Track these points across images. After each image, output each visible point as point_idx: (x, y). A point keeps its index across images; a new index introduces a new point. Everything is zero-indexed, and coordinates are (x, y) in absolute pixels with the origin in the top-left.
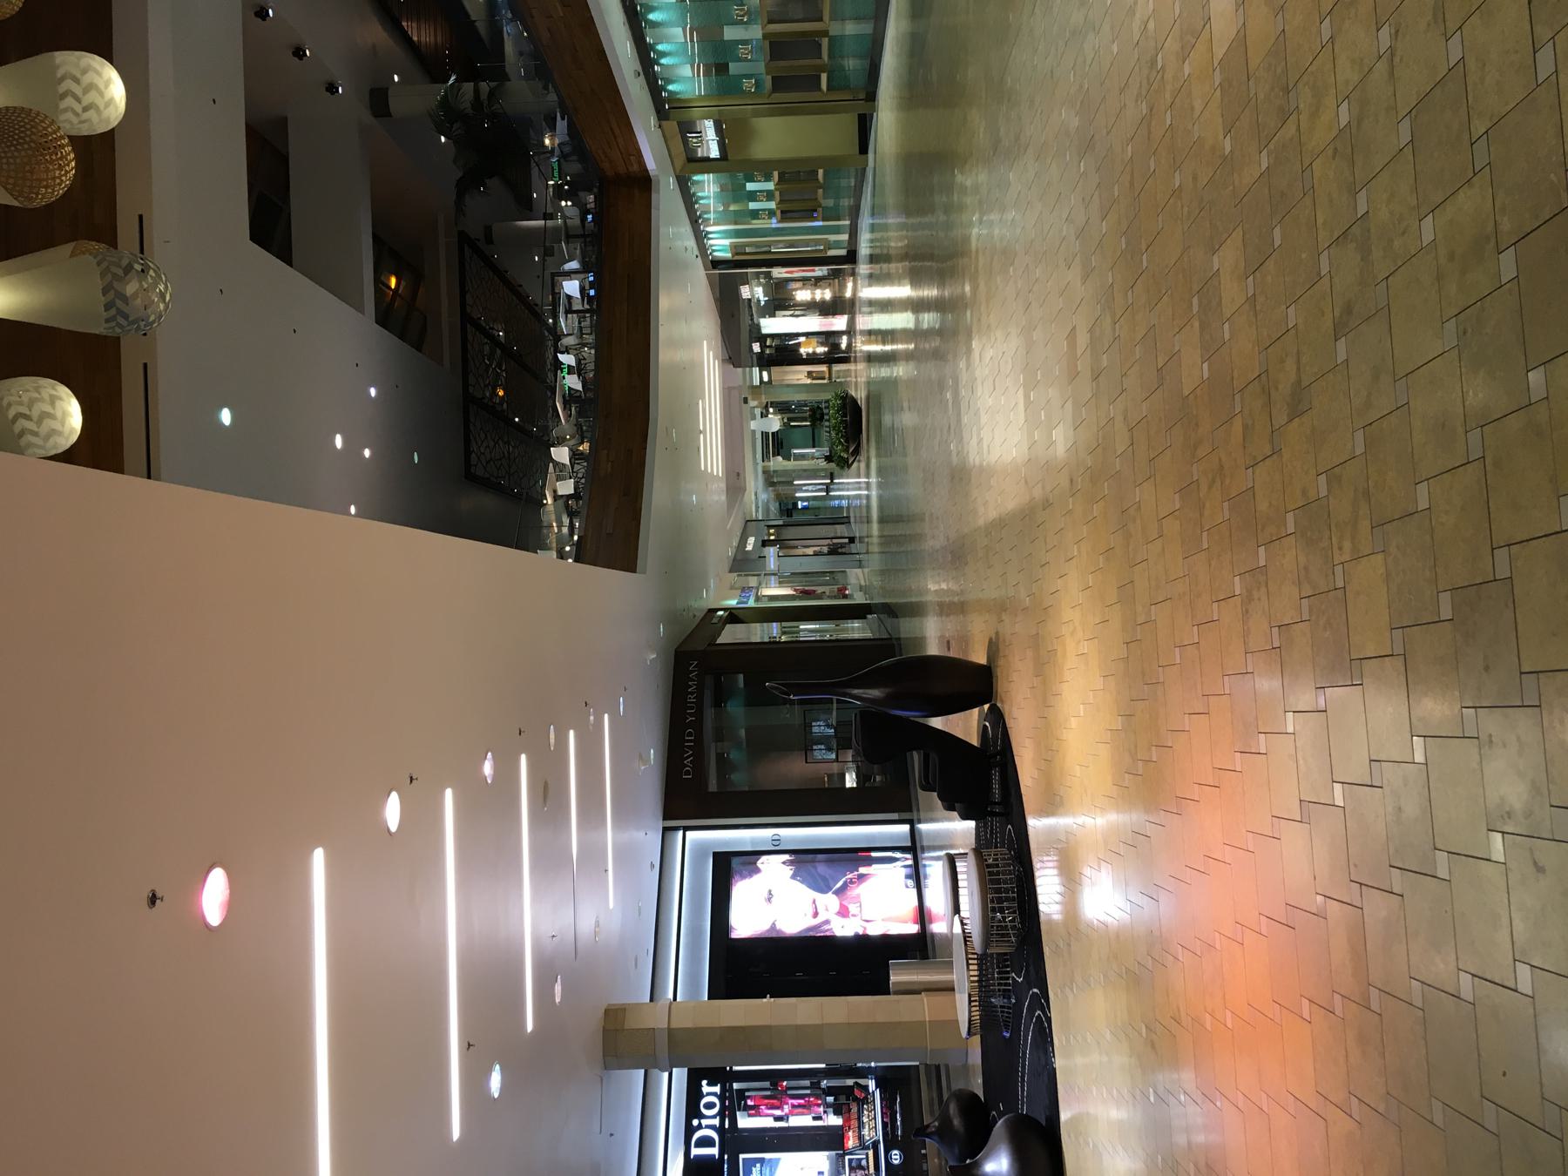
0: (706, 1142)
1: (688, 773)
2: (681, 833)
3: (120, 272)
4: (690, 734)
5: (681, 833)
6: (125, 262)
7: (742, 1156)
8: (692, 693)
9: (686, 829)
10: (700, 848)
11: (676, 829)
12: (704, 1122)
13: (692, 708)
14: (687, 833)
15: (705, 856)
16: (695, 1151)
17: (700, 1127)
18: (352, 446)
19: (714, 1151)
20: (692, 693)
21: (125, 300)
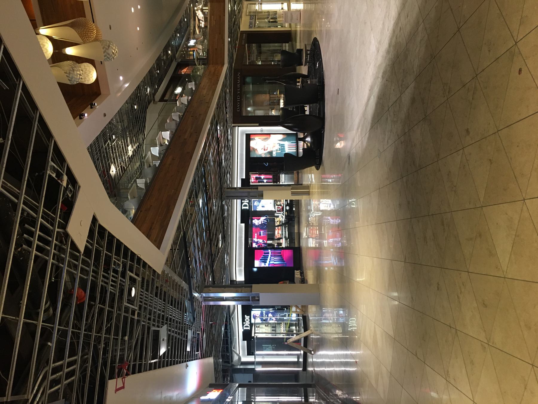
0: (245, 206)
1: (238, 110)
2: (237, 127)
3: (107, 47)
4: (238, 97)
5: (237, 127)
6: (108, 45)
7: (252, 200)
8: (239, 84)
9: (238, 126)
10: (242, 133)
11: (236, 126)
12: (245, 201)
13: (239, 89)
14: (239, 128)
15: (244, 135)
16: (243, 208)
17: (244, 202)
18: (136, 8)
19: (247, 208)
20: (239, 84)
21: (109, 54)
